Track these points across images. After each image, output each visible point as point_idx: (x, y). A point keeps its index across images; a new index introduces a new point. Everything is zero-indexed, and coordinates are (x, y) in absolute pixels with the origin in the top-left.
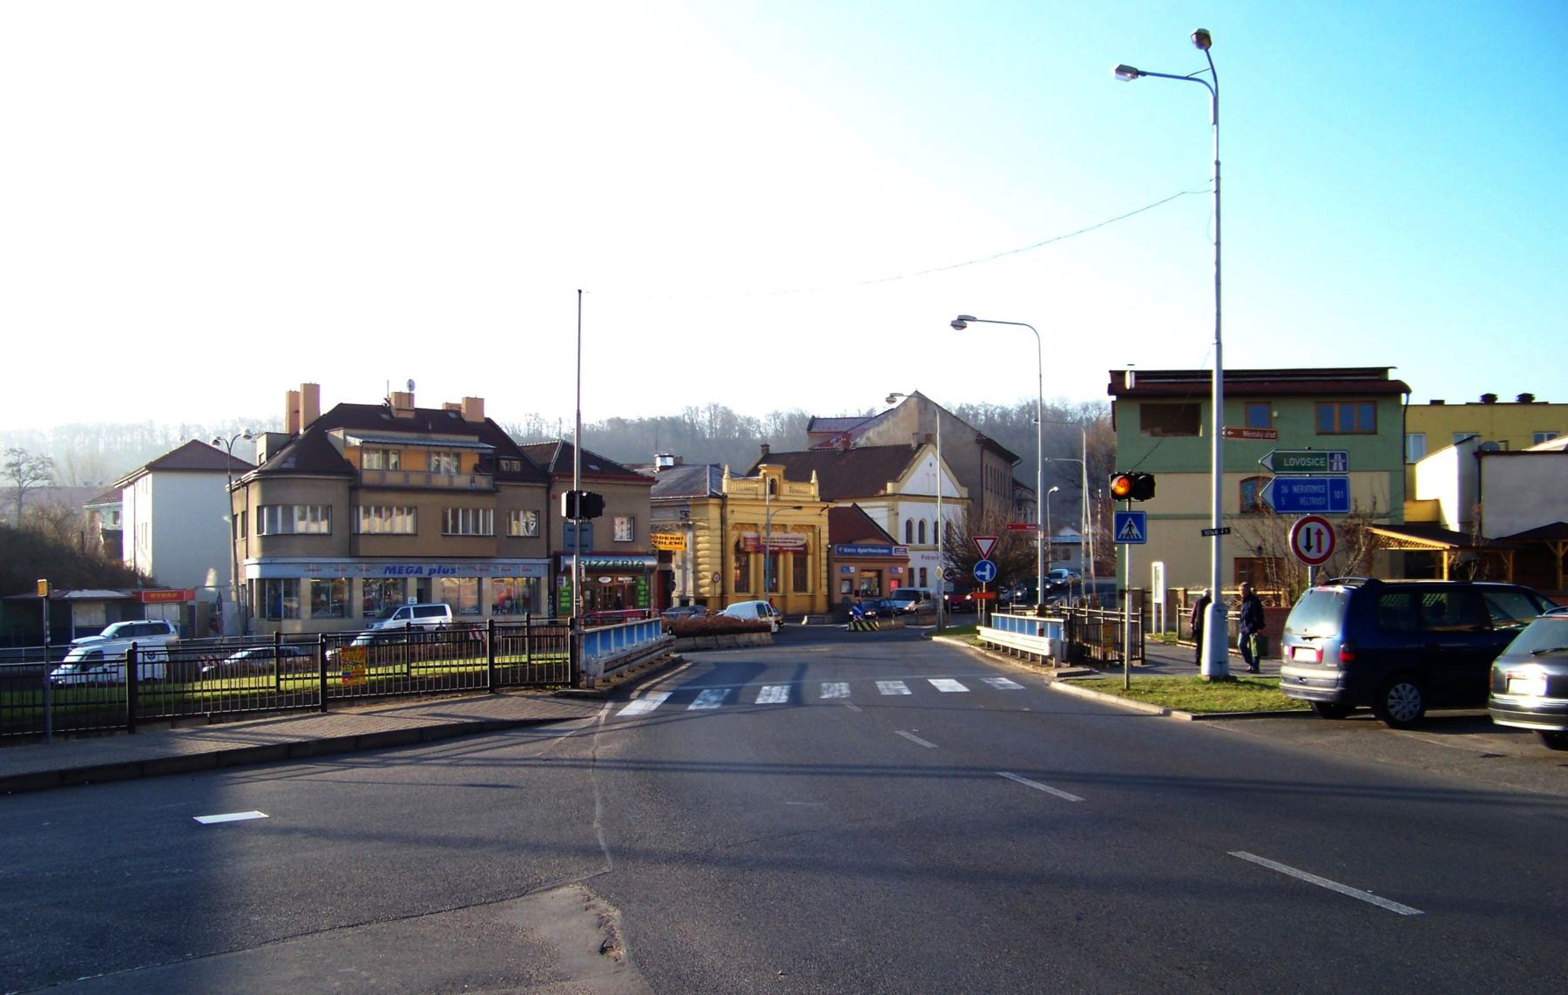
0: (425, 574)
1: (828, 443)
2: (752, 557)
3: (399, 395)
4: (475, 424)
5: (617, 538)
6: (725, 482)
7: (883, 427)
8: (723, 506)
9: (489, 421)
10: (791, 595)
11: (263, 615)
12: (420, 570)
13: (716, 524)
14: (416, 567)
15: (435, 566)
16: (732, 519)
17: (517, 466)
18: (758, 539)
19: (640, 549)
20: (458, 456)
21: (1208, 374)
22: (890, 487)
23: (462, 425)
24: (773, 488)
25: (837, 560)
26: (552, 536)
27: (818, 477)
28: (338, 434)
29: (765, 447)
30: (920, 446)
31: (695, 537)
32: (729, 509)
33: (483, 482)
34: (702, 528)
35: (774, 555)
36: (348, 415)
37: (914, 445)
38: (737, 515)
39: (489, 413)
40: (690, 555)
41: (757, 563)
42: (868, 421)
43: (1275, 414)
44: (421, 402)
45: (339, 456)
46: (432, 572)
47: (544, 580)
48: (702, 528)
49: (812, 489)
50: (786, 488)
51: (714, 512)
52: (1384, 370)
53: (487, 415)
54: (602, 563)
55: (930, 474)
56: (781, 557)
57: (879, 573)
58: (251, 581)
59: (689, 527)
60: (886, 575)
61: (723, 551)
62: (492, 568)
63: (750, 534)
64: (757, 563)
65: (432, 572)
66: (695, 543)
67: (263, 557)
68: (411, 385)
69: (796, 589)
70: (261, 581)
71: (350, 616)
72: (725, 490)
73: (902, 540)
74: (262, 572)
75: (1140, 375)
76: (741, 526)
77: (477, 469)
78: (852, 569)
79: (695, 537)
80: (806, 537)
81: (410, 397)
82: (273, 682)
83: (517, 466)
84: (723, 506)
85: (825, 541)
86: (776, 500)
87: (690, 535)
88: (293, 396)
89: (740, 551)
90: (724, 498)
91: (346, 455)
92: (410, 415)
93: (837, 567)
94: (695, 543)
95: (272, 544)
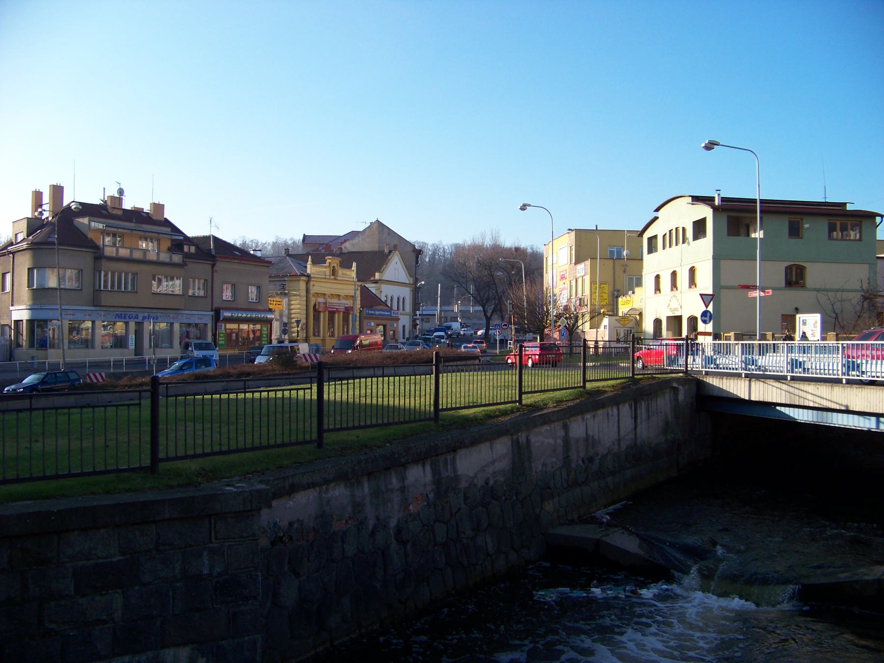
0: (140, 320)
1: (317, 250)
2: (322, 314)
3: (112, 198)
4: (161, 221)
5: (224, 298)
6: (309, 266)
7: (355, 241)
8: (308, 283)
9: (166, 220)
10: (328, 339)
11: (31, 345)
12: (137, 317)
13: (304, 293)
14: (134, 314)
15: (146, 314)
16: (313, 290)
17: (193, 249)
18: (325, 303)
19: (260, 308)
20: (158, 240)
21: (754, 201)
22: (377, 276)
23: (151, 222)
24: (334, 272)
25: (366, 318)
26: (215, 299)
27: (357, 267)
28: (85, 220)
29: (287, 250)
30: (390, 252)
31: (289, 301)
32: (312, 283)
33: (177, 258)
34: (295, 295)
35: (332, 314)
36: (87, 209)
37: (386, 251)
38: (315, 288)
39: (168, 215)
40: (286, 312)
41: (323, 317)
42: (354, 234)
43: (806, 226)
44: (128, 204)
45: (86, 237)
46: (144, 318)
47: (210, 326)
48: (295, 295)
49: (353, 273)
50: (341, 272)
51: (303, 285)
52: (844, 204)
53: (165, 216)
54: (244, 315)
55: (395, 269)
56: (336, 315)
57: (385, 326)
58: (17, 322)
59: (286, 294)
60: (388, 327)
61: (307, 310)
62: (180, 317)
63: (321, 300)
64: (323, 317)
65: (144, 318)
66: (289, 305)
67: (34, 304)
68: (121, 192)
69: (314, 335)
70: (31, 322)
71: (93, 347)
72: (308, 271)
73: (395, 308)
74: (32, 315)
75: (723, 200)
76: (317, 295)
77: (169, 250)
78: (373, 324)
79: (289, 301)
80: (349, 303)
81: (120, 200)
82: (627, 422)
83: (193, 249)
84: (308, 283)
85: (358, 305)
86: (335, 279)
87: (285, 300)
88: (38, 196)
89: (317, 312)
90: (309, 276)
91: (90, 236)
92: (120, 213)
93: (365, 322)
94: (289, 305)
95: (40, 295)
